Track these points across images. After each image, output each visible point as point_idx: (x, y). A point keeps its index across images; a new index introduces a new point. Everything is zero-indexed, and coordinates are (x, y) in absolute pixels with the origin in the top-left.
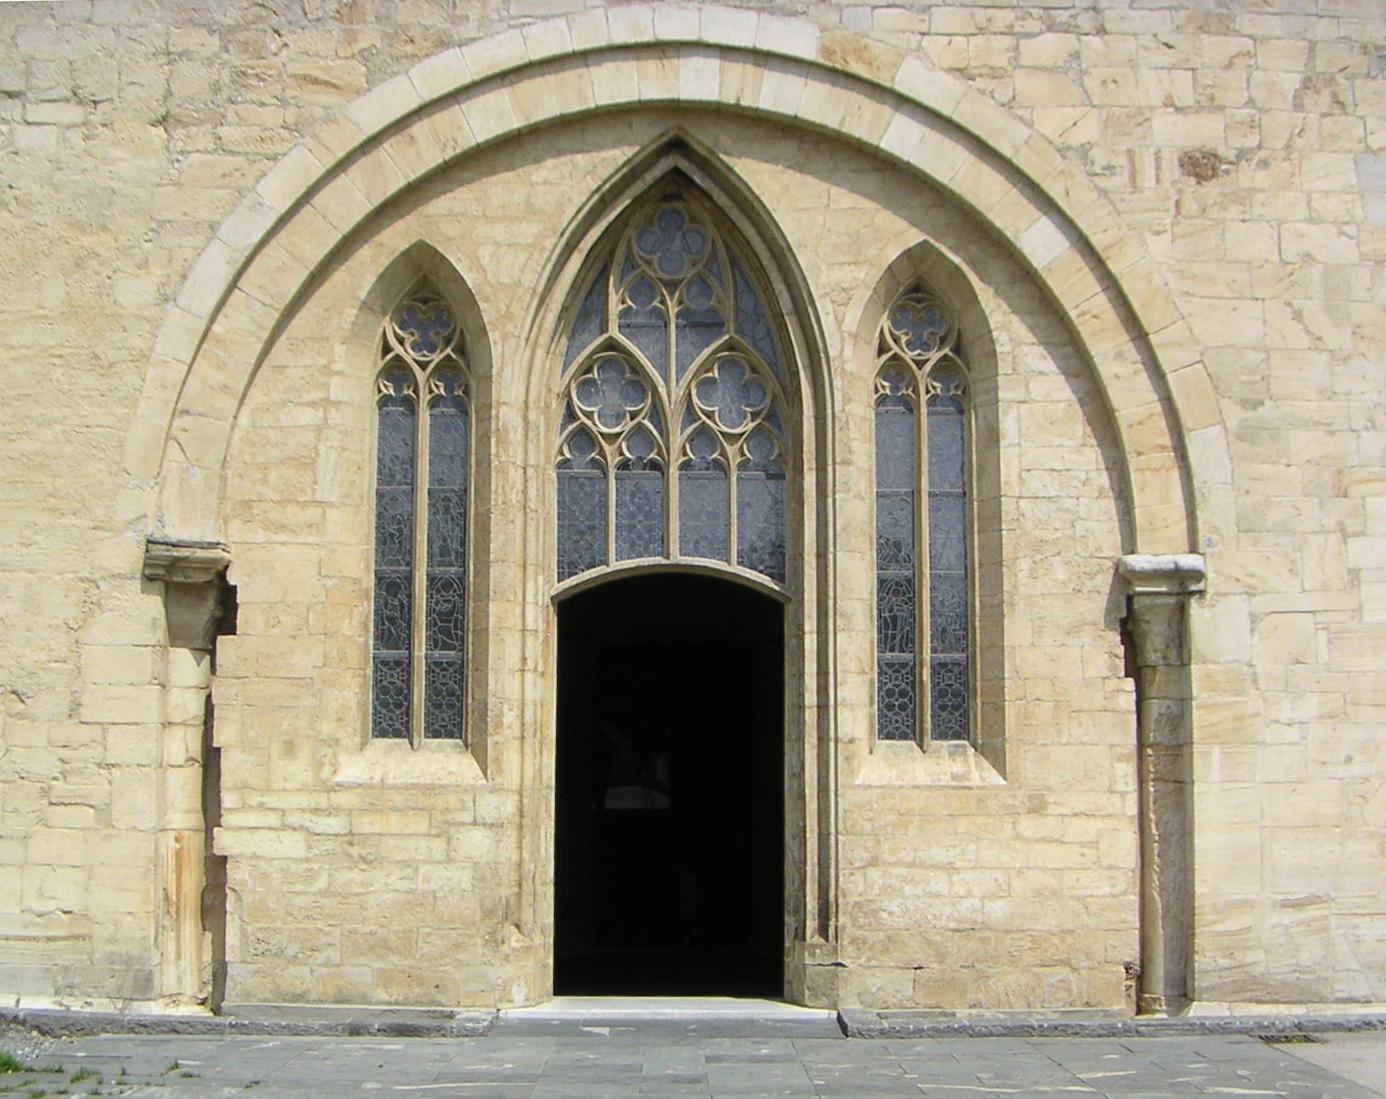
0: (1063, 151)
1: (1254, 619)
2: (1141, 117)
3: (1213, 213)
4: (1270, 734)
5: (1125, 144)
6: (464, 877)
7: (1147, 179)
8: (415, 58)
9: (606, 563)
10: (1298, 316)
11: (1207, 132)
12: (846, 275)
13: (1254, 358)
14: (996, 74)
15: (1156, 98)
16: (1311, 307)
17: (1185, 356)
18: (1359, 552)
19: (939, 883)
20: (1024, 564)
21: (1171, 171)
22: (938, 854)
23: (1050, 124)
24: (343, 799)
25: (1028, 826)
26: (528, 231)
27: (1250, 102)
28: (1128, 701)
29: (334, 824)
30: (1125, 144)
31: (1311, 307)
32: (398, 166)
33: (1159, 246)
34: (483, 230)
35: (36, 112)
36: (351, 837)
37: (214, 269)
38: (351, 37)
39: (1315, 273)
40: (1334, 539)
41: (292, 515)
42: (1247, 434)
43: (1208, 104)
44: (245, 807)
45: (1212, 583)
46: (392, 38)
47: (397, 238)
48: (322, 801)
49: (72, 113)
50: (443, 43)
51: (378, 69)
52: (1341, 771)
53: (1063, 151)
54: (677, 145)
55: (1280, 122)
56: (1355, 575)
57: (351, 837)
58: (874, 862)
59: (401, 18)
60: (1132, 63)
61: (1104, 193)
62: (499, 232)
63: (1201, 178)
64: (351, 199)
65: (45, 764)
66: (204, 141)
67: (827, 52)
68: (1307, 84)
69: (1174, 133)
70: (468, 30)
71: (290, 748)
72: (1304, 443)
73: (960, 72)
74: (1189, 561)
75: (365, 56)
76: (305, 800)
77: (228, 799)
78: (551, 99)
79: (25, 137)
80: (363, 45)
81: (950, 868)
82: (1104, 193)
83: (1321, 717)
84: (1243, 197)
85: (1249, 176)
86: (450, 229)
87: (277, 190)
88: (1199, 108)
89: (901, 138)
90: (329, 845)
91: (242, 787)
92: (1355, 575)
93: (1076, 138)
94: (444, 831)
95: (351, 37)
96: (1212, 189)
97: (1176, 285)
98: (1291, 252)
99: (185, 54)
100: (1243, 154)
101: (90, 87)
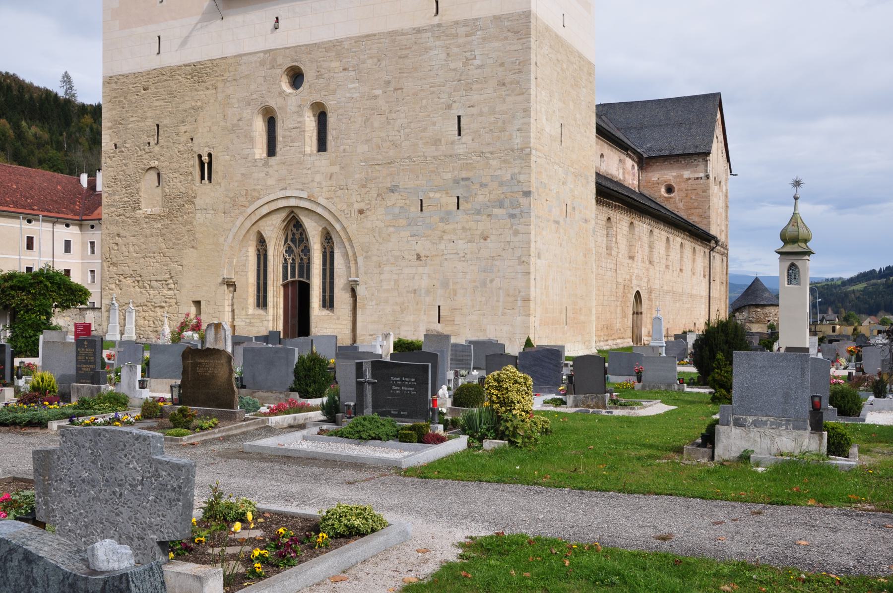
0: (341, 211)
1: (366, 288)
2: (352, 204)
3: (362, 220)
4: (368, 307)
5: (350, 209)
6: (264, 328)
7: (353, 215)
8: (255, 201)
9: (287, 279)
10: (374, 237)
11: (362, 206)
12: (314, 233)
13: (367, 244)
14: (332, 198)
15: (355, 200)
16: (376, 235)
17: (357, 245)
18: (382, 277)
19: (325, 331)
20: (337, 280)
21: (356, 213)
22: (325, 326)
23: (339, 207)
24: (249, 317)
25: (337, 321)
26: (272, 228)
27: (369, 200)
28: (352, 302)
29: (248, 321)
30: (350, 209)
31: (376, 235)
32: (254, 218)
33: (354, 226)
34: (266, 228)
35: (209, 212)
36: (250, 323)
37: (231, 236)
38: (247, 198)
39: (377, 229)
40: (378, 275)
41: (243, 273)
42: (366, 257)
43: (363, 201)
44: (238, 318)
45: (360, 282)
46: (252, 198)
47: (255, 229)
48: (247, 317)
49: (213, 212)
50: (258, 199)
51: (251, 202)
52: (379, 313)
53: (341, 211)
54: (292, 212)
55: (374, 202)
56: (381, 280)
57: (250, 323)
58: (316, 327)
59: (253, 195)
60: (351, 195)
61: (346, 218)
62: (268, 228)
63: (361, 214)
64: (248, 224)
65: (212, 311)
66: (229, 216)
67: (308, 197)
68: (378, 195)
69: (357, 206)
70: (261, 196)
71: (243, 309)
72: (375, 259)
73: (327, 199)
74: (357, 279)
75: (249, 201)
76: (245, 317)
77: (235, 317)
78: (273, 206)
79: (208, 216)
80: (248, 199)
81: (326, 328)
82: (346, 218)
83: (376, 304)
84: (366, 217)
85: (368, 213)
86: (262, 228)
87: (238, 223)
88: (361, 201)
89: (319, 210)
90: (248, 324)
91: (237, 315)
92: (381, 280)
93: (343, 208)
94: (262, 321)
95: (247, 198)
96: (362, 216)
97: (356, 233)
98: (374, 226)
99: (226, 202)
100: (367, 209)
101: (215, 208)
